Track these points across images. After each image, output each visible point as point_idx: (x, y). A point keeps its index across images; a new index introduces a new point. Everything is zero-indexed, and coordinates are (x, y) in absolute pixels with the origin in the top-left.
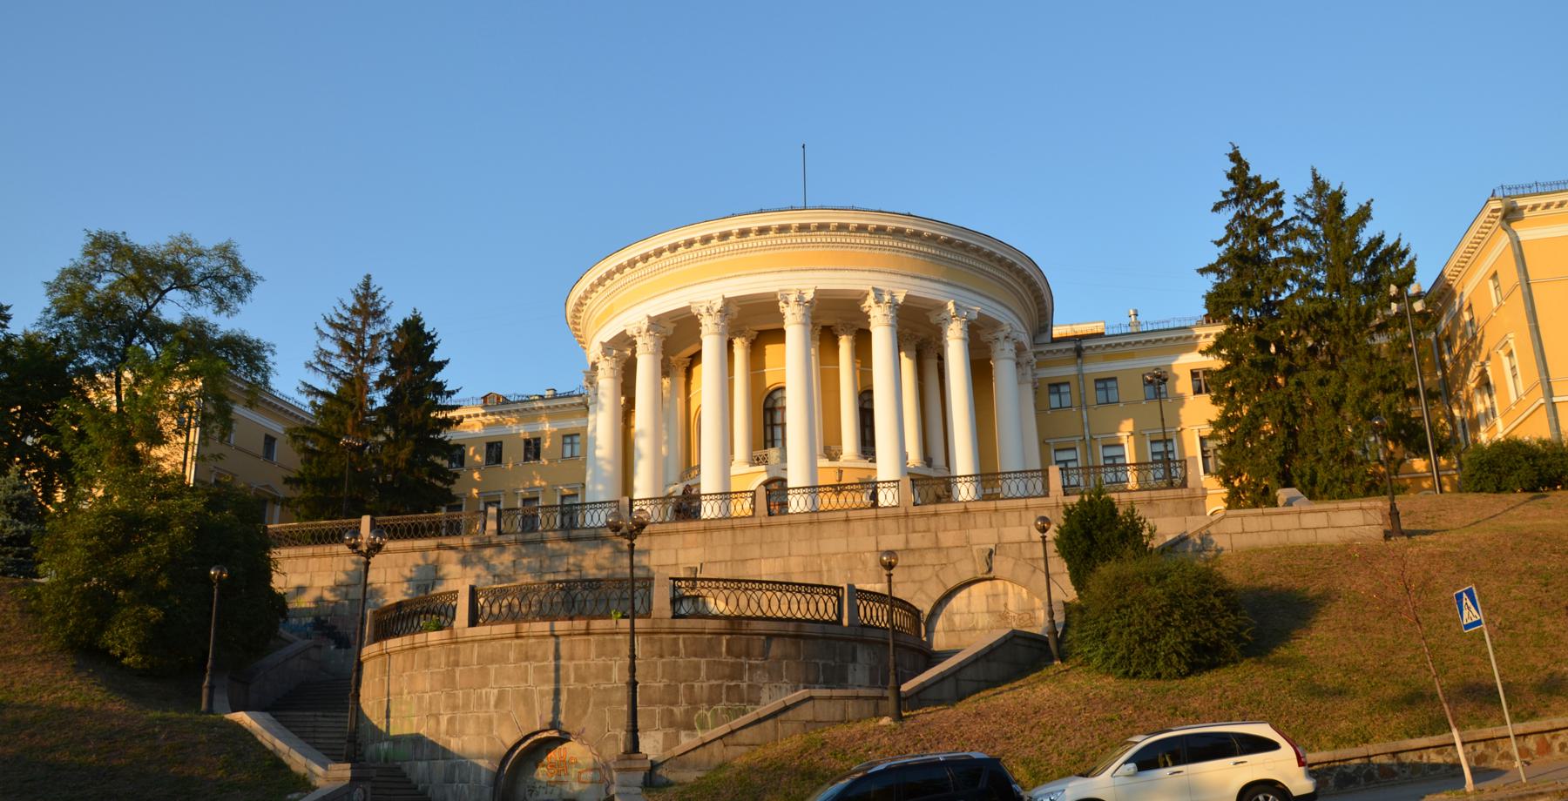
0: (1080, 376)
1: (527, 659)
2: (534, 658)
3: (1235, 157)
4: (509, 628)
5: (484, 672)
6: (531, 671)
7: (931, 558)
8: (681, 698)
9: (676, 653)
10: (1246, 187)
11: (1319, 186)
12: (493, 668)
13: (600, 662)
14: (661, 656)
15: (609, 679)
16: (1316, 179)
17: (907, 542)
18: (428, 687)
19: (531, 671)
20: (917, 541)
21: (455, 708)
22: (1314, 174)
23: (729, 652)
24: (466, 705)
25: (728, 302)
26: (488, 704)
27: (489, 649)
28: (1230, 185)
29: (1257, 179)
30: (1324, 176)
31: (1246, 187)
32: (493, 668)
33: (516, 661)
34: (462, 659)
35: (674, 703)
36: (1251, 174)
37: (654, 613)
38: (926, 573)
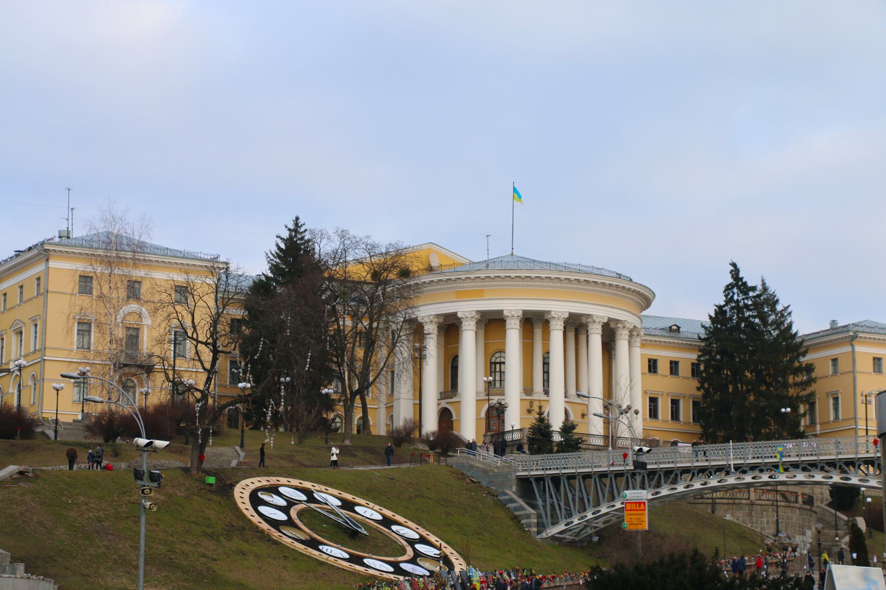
3: (734, 265)
5: (762, 514)
10: (737, 282)
11: (765, 289)
12: (765, 513)
16: (764, 284)
21: (752, 523)
22: (763, 280)
24: (757, 523)
25: (571, 314)
27: (763, 507)
28: (731, 280)
29: (742, 278)
30: (768, 284)
31: (737, 282)
32: (765, 513)
36: (741, 276)
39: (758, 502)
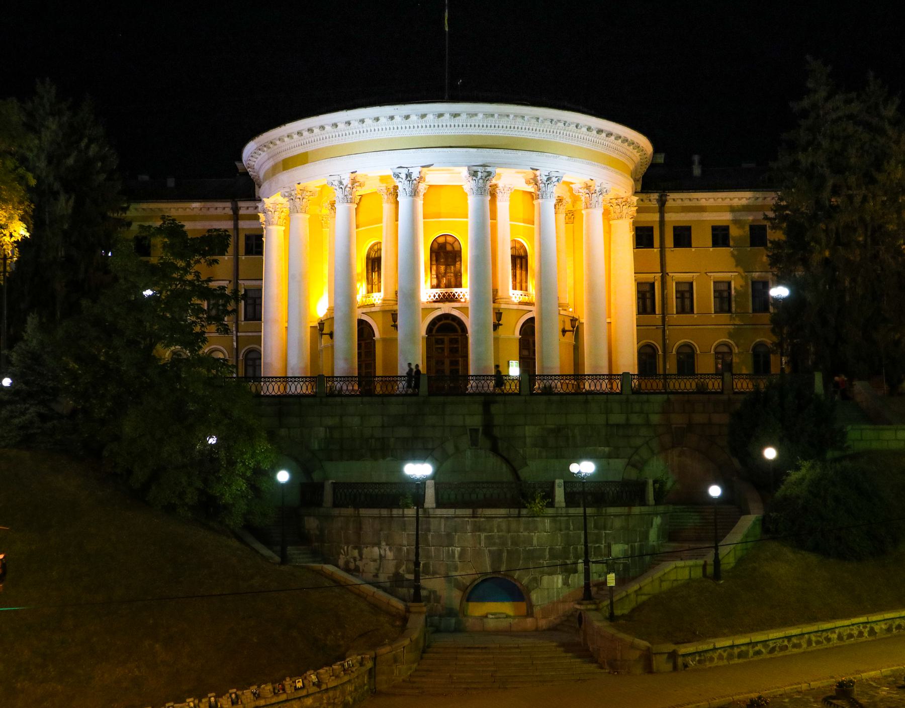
0: (662, 222)
1: (479, 531)
2: (484, 530)
4: (468, 512)
6: (483, 537)
7: (643, 431)
8: (571, 555)
9: (568, 528)
13: (526, 534)
14: (561, 530)
15: (532, 545)
17: (627, 419)
18: (405, 542)
19: (483, 537)
20: (635, 419)
23: (596, 527)
26: (454, 557)
33: (473, 531)
34: (432, 528)
35: (568, 558)
37: (557, 505)
38: (638, 442)
39: (439, 512)
